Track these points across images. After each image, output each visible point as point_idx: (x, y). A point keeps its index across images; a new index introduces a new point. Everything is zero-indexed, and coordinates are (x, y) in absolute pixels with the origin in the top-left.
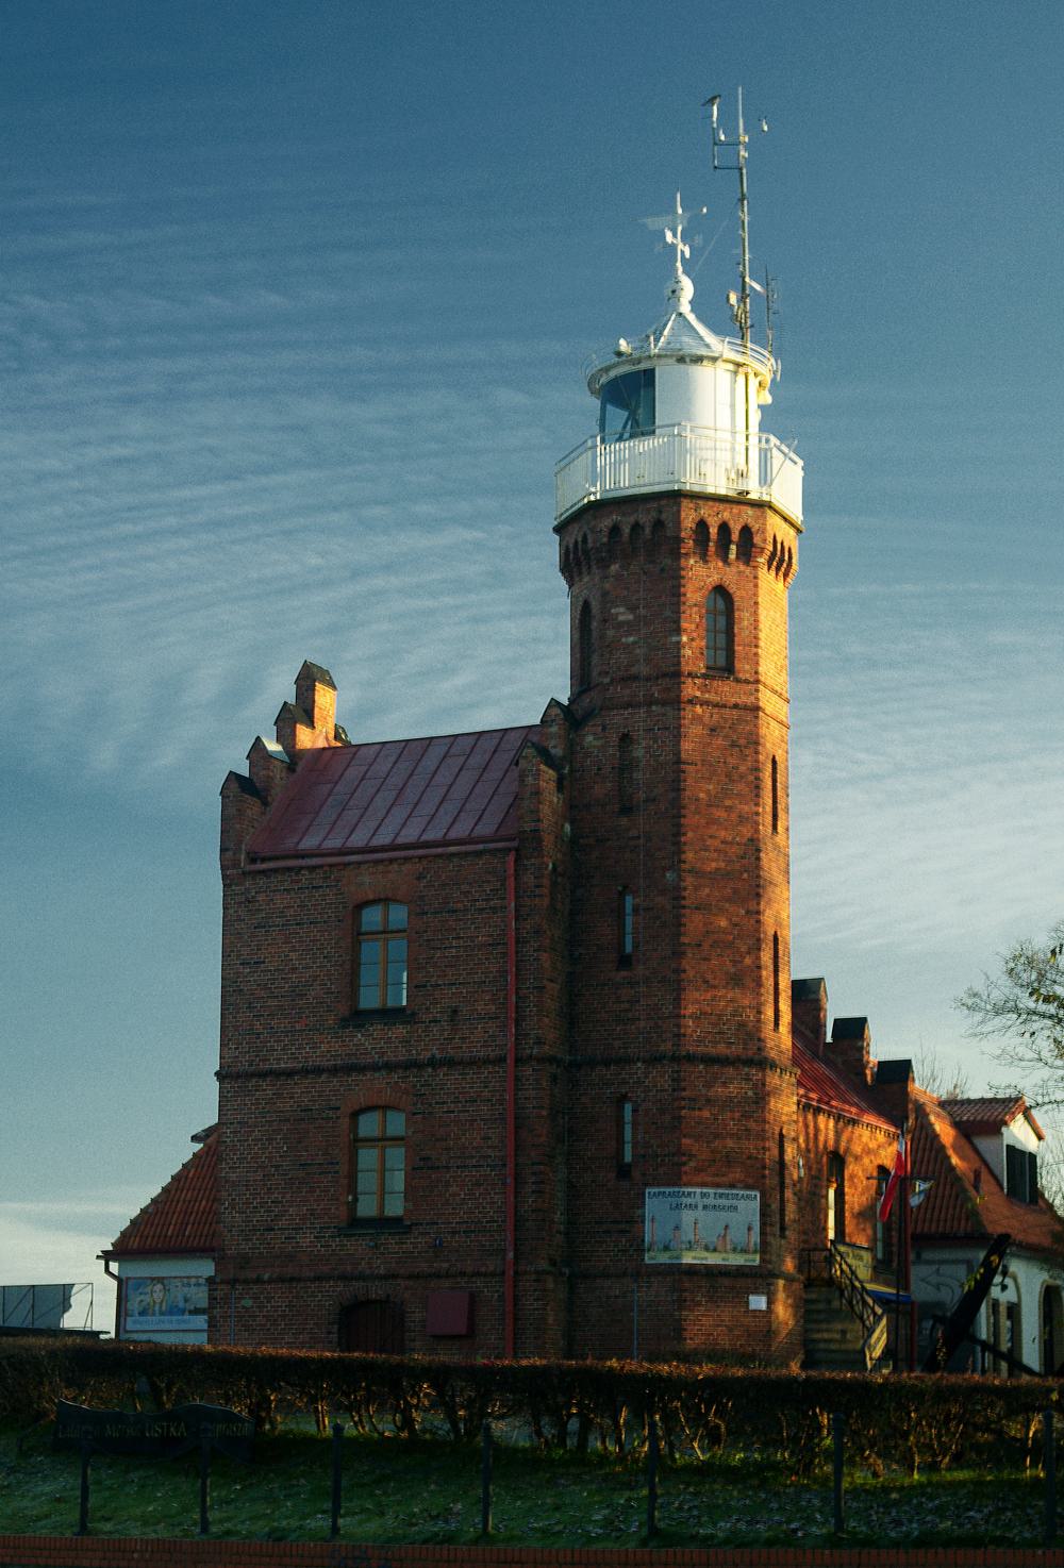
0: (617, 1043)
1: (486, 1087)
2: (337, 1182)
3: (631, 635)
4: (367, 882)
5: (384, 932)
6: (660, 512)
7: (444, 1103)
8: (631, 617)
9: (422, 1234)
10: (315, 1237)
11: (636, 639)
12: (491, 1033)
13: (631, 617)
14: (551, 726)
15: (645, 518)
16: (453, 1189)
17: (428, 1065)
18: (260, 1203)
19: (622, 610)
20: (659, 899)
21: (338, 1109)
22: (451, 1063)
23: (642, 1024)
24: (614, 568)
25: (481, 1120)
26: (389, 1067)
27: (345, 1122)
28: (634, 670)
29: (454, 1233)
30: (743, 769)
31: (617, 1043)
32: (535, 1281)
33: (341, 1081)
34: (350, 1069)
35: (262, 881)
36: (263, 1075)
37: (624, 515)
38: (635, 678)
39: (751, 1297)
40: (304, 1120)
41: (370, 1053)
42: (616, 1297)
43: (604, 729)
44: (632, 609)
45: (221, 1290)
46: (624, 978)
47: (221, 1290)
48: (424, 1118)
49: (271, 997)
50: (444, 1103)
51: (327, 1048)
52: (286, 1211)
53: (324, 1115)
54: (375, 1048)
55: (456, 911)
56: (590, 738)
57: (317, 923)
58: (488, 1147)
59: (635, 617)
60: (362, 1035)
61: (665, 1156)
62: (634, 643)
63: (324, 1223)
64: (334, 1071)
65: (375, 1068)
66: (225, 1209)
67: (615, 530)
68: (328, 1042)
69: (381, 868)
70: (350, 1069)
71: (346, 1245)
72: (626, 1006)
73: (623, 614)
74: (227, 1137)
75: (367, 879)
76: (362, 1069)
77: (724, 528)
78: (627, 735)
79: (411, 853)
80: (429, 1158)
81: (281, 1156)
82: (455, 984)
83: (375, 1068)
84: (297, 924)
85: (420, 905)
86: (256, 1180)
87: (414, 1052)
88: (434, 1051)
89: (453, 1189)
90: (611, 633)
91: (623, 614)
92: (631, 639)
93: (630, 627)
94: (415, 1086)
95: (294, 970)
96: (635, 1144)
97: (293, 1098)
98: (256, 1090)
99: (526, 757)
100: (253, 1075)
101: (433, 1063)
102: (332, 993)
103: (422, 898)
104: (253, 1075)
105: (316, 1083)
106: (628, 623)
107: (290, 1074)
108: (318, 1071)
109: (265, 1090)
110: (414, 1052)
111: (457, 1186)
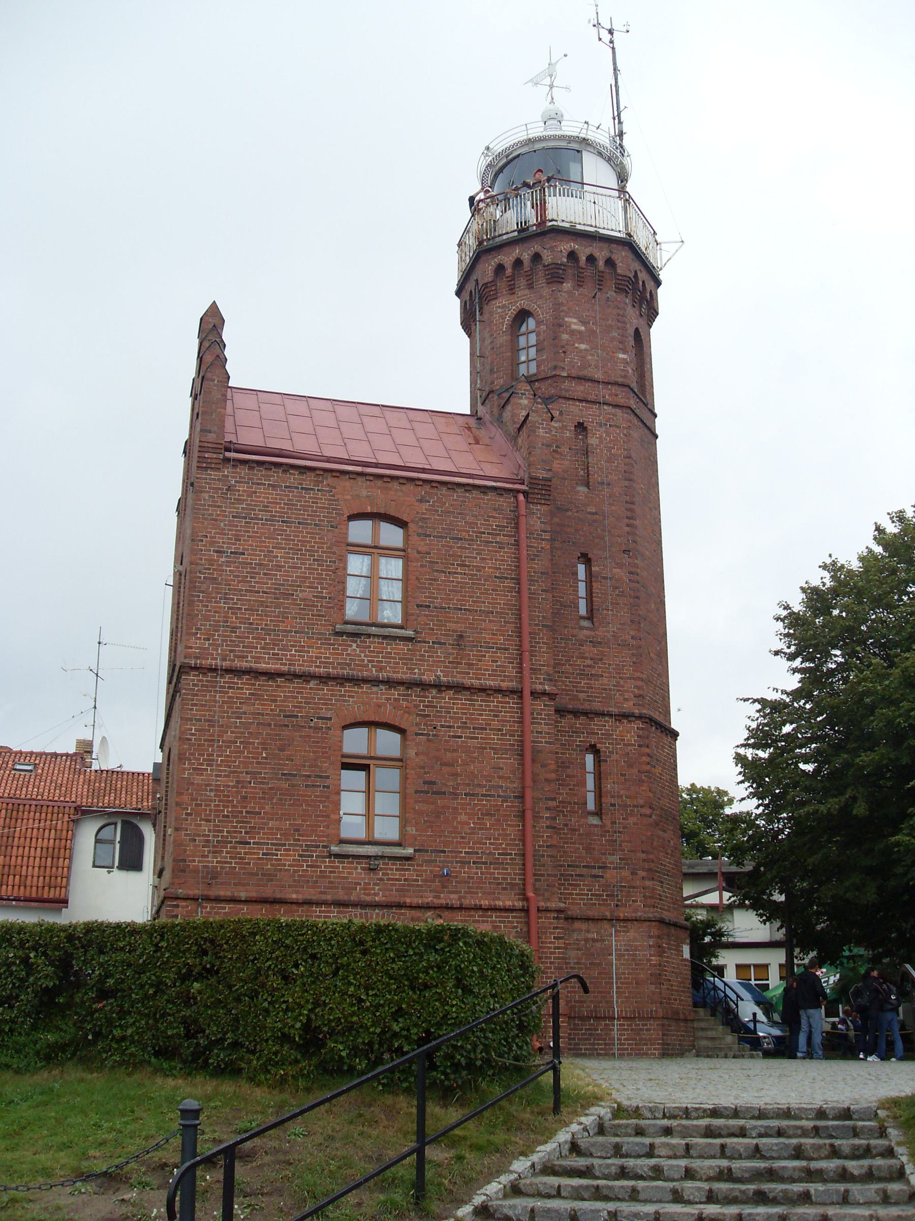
1: (497, 716)
2: (328, 797)
5: (376, 547)
9: (426, 861)
10: (300, 855)
11: (588, 347)
13: (583, 328)
14: (521, 398)
16: (463, 817)
18: (232, 812)
19: (575, 321)
21: (330, 719)
22: (459, 688)
24: (567, 286)
25: (493, 749)
26: (391, 683)
29: (463, 863)
31: (582, 696)
32: (554, 918)
33: (333, 690)
35: (243, 471)
40: (287, 726)
44: (584, 323)
45: (183, 907)
46: (587, 637)
47: (183, 907)
48: (429, 740)
49: (251, 591)
50: (450, 727)
51: (317, 657)
52: (264, 824)
54: (373, 661)
55: (461, 539)
57: (307, 524)
58: (499, 777)
59: (586, 330)
61: (634, 806)
62: (586, 350)
63: (311, 841)
64: (324, 679)
65: (376, 682)
66: (187, 814)
67: (572, 255)
68: (317, 648)
69: (379, 483)
71: (338, 867)
72: (589, 662)
76: (357, 681)
78: (583, 424)
81: (258, 763)
82: (461, 609)
83: (376, 682)
84: (282, 521)
85: (422, 527)
86: (228, 786)
87: (416, 671)
89: (463, 817)
90: (565, 337)
92: (583, 346)
94: (417, 706)
95: (279, 567)
97: (276, 701)
98: (229, 688)
101: (439, 686)
102: (322, 597)
104: (229, 671)
105: (306, 688)
106: (580, 332)
107: (271, 675)
108: (307, 677)
109: (242, 689)
110: (416, 671)
111: (466, 814)
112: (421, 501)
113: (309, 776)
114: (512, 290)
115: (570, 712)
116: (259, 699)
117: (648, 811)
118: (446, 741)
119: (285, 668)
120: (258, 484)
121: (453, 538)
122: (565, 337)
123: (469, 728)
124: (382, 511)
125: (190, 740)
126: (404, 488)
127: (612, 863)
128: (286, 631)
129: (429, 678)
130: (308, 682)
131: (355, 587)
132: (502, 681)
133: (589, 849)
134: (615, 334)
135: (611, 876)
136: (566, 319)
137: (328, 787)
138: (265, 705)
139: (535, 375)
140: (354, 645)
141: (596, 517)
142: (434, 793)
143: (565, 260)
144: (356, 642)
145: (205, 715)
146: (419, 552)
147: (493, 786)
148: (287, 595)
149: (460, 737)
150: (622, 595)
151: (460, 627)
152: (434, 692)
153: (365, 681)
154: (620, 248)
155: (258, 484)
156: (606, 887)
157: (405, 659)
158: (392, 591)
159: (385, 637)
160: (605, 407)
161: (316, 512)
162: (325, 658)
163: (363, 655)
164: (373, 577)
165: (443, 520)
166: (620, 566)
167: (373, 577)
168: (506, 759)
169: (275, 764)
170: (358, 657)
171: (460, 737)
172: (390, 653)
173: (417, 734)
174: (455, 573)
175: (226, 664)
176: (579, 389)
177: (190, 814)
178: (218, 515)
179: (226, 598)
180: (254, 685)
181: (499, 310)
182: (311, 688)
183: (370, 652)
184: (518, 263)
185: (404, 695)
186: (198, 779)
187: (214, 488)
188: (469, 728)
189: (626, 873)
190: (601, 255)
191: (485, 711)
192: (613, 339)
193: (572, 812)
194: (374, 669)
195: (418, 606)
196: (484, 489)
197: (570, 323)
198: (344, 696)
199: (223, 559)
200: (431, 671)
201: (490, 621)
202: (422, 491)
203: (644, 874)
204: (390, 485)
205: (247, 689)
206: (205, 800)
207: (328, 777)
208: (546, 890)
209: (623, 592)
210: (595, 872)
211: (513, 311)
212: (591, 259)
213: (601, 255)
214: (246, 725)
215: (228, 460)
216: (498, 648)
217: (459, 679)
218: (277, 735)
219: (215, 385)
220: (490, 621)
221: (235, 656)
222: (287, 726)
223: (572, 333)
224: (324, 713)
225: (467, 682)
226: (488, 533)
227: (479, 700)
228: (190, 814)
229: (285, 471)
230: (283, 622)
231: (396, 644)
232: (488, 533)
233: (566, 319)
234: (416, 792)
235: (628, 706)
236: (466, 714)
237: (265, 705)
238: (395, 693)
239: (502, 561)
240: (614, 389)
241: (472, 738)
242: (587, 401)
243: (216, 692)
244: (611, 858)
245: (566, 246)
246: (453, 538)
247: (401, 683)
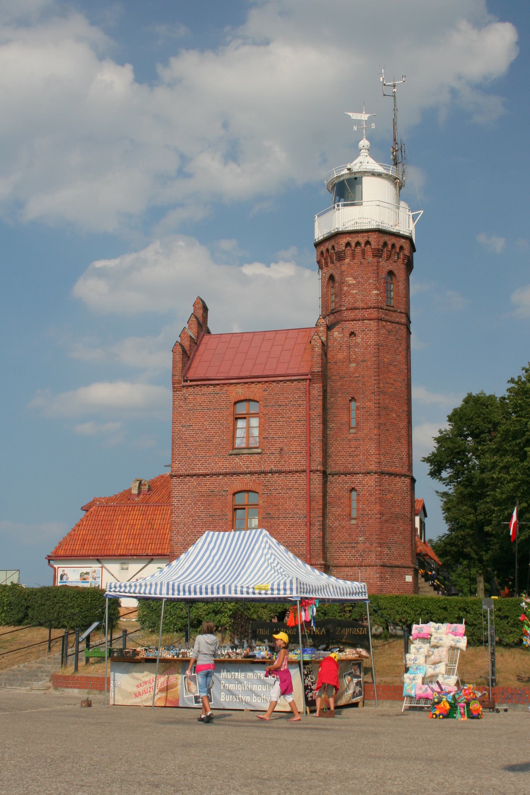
0: (349, 466)
3: (355, 290)
4: (240, 391)
6: (369, 237)
8: (355, 282)
11: (357, 291)
13: (355, 282)
15: (362, 239)
16: (282, 527)
17: (270, 473)
19: (350, 279)
20: (368, 404)
21: (227, 491)
22: (280, 472)
23: (361, 457)
24: (347, 261)
26: (251, 473)
27: (230, 497)
28: (356, 305)
30: (400, 349)
34: (232, 474)
35: (191, 390)
36: (192, 476)
37: (352, 238)
38: (355, 309)
39: (407, 576)
42: (351, 575)
43: (343, 329)
44: (355, 279)
56: (336, 333)
58: (297, 509)
64: (225, 474)
65: (245, 473)
67: (348, 244)
69: (247, 385)
70: (232, 474)
73: (350, 280)
75: (240, 391)
77: (393, 246)
79: (260, 380)
80: (270, 514)
83: (245, 473)
89: (282, 527)
90: (345, 288)
91: (350, 280)
92: (354, 292)
96: (358, 509)
99: (314, 339)
100: (188, 476)
103: (266, 399)
104: (188, 476)
106: (353, 284)
107: (204, 475)
108: (218, 475)
115: (342, 474)
117: (377, 516)
119: (209, 472)
124: (248, 398)
126: (257, 386)
127: (361, 541)
129: (267, 469)
130: (219, 476)
131: (240, 433)
133: (350, 535)
134: (371, 281)
135: (361, 547)
139: (334, 309)
140: (237, 459)
141: (358, 379)
142: (270, 518)
143: (344, 248)
146: (264, 414)
147: (295, 513)
148: (210, 441)
150: (371, 415)
151: (282, 445)
152: (270, 475)
156: (357, 551)
158: (256, 432)
159: (249, 454)
160: (365, 321)
164: (248, 428)
166: (370, 401)
167: (248, 428)
170: (240, 463)
175: (186, 473)
176: (351, 315)
184: (327, 250)
189: (368, 544)
190: (362, 241)
192: (370, 284)
193: (343, 519)
195: (263, 438)
196: (292, 381)
197: (348, 281)
201: (294, 441)
202: (265, 386)
203: (377, 545)
204: (250, 386)
208: (317, 556)
210: (353, 545)
212: (358, 244)
213: (362, 241)
214: (195, 497)
216: (298, 453)
217: (280, 468)
219: (177, 354)
220: (294, 441)
223: (349, 285)
224: (225, 489)
225: (284, 469)
227: (289, 476)
229: (208, 387)
233: (346, 279)
234: (263, 518)
235: (373, 467)
238: (254, 477)
240: (370, 311)
242: (356, 321)
244: (361, 539)
245: (344, 241)
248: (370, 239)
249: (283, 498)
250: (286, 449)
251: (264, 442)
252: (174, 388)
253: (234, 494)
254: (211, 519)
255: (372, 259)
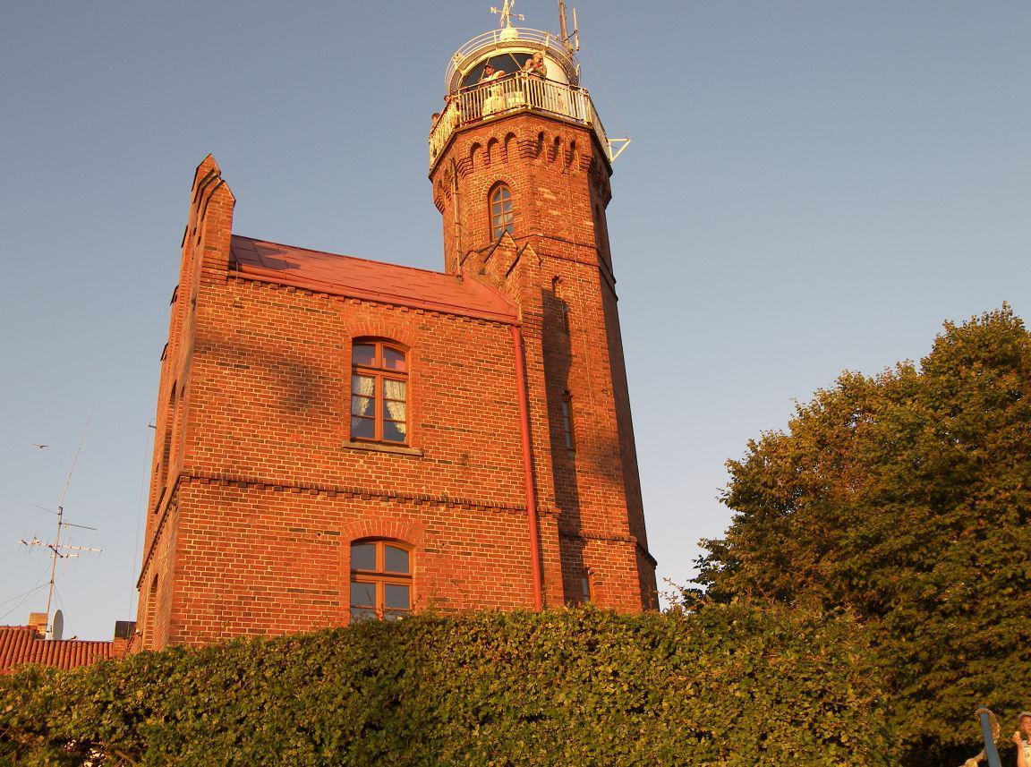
1: (504, 534)
7: (459, 543)
11: (560, 214)
12: (503, 483)
13: (554, 198)
21: (338, 534)
22: (469, 505)
24: (538, 162)
25: (502, 566)
27: (344, 552)
33: (340, 505)
34: (353, 494)
37: (548, 127)
40: (294, 540)
41: (375, 482)
44: (556, 193)
50: (459, 543)
53: (320, 538)
54: (380, 477)
60: (365, 462)
64: (335, 493)
66: (184, 633)
68: (324, 462)
70: (353, 494)
74: (191, 547)
75: (368, 317)
81: (262, 578)
82: (464, 431)
87: (424, 488)
88: (446, 491)
90: (539, 203)
92: (555, 213)
93: (554, 205)
101: (450, 503)
102: (329, 413)
112: (423, 328)
113: (317, 592)
114: (487, 163)
116: (264, 512)
118: (455, 558)
120: (263, 302)
121: (454, 364)
122: (539, 203)
123: (477, 545)
125: (189, 553)
128: (291, 445)
130: (315, 495)
132: (508, 500)
136: (539, 189)
137: (337, 604)
138: (270, 518)
140: (361, 461)
144: (362, 458)
145: (205, 528)
149: (470, 554)
152: (443, 508)
153: (372, 495)
154: (583, 133)
155: (263, 302)
157: (412, 476)
160: (577, 265)
161: (321, 332)
162: (332, 472)
163: (370, 471)
165: (444, 347)
168: (515, 576)
169: (280, 579)
171: (470, 554)
172: (397, 470)
173: (429, 551)
174: (460, 397)
177: (187, 633)
178: (221, 329)
179: (229, 410)
180: (258, 497)
181: (476, 182)
182: (318, 503)
183: (378, 468)
184: (493, 141)
185: (412, 511)
186: (196, 595)
187: (217, 303)
188: (477, 545)
191: (492, 528)
194: (382, 486)
195: (423, 425)
198: (353, 511)
199: (227, 372)
200: (438, 488)
205: (251, 501)
206: (204, 618)
207: (337, 593)
209: (604, 427)
211: (489, 183)
215: (234, 278)
218: (282, 549)
221: (238, 467)
222: (294, 540)
223: (545, 200)
224: (332, 527)
225: (474, 500)
226: (487, 362)
227: (486, 519)
228: (187, 633)
230: (289, 435)
231: (403, 462)
232: (487, 362)
233: (539, 189)
236: (473, 531)
237: (270, 518)
239: (501, 387)
241: (481, 555)
243: (218, 503)
246: (454, 364)
247: (408, 499)
248: (578, 140)
249: (474, 565)
250: (474, 456)
251: (424, 434)
252: (205, 274)
253: (354, 543)
254: (292, 601)
255: (578, 171)
